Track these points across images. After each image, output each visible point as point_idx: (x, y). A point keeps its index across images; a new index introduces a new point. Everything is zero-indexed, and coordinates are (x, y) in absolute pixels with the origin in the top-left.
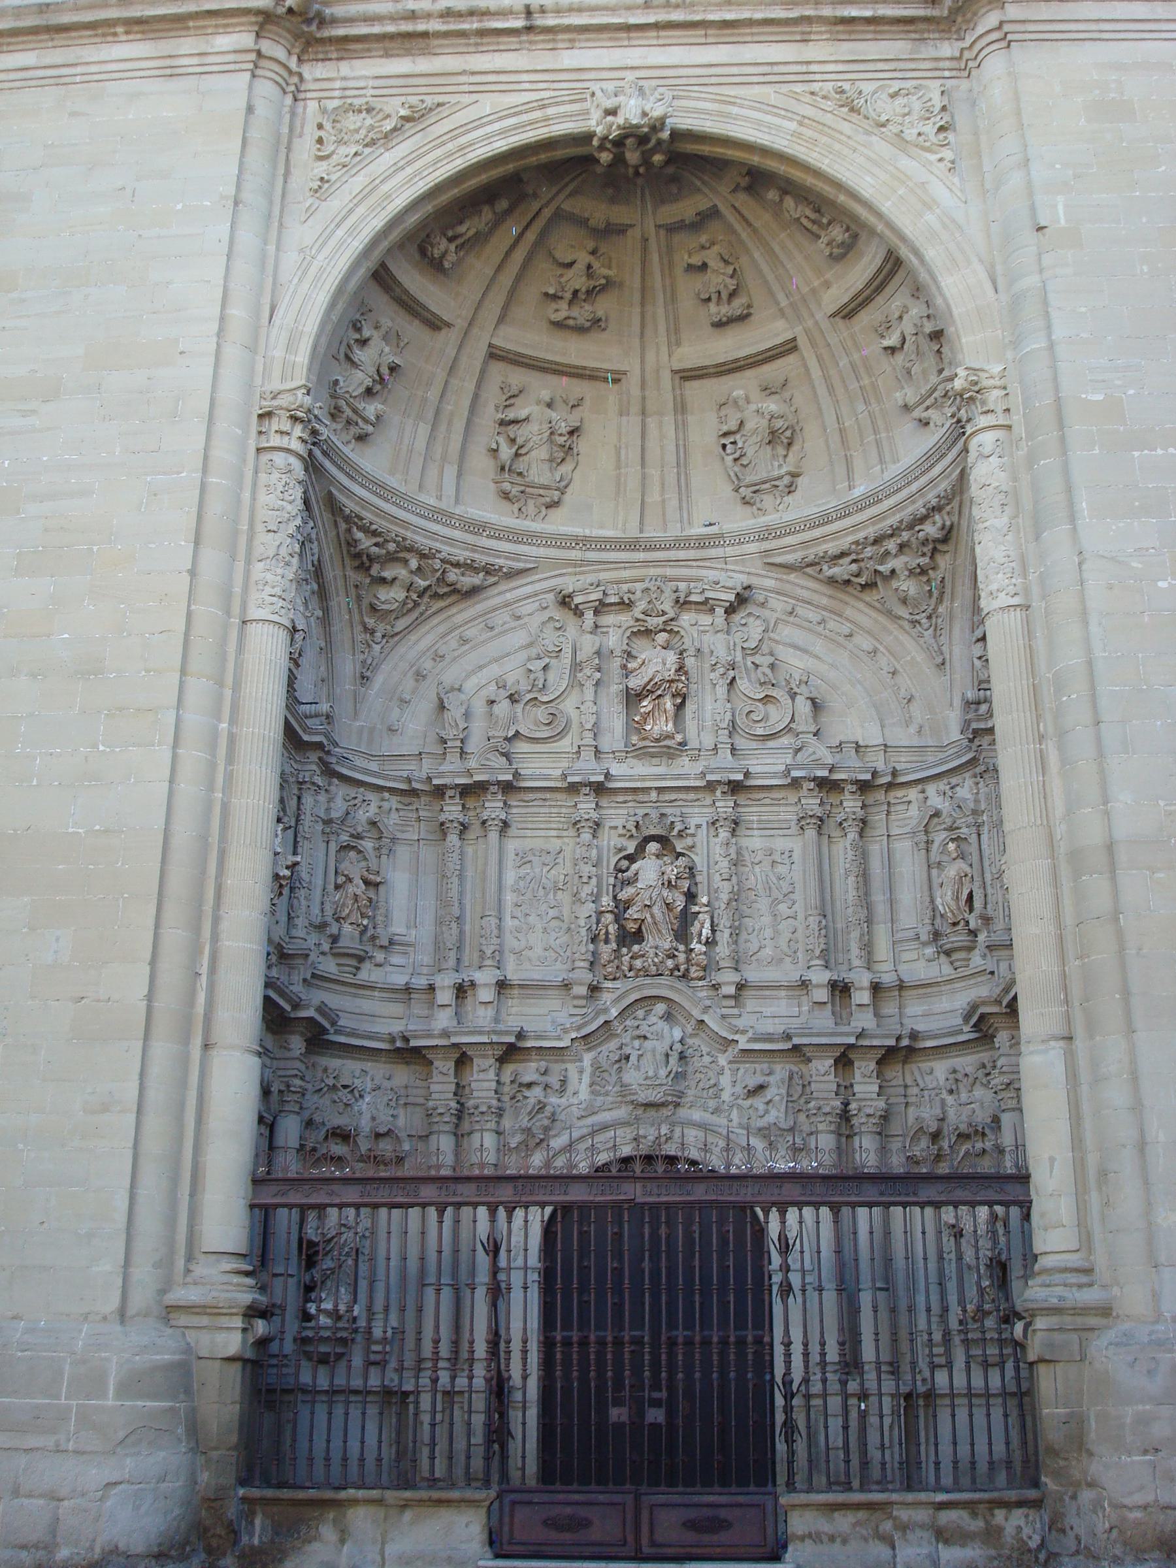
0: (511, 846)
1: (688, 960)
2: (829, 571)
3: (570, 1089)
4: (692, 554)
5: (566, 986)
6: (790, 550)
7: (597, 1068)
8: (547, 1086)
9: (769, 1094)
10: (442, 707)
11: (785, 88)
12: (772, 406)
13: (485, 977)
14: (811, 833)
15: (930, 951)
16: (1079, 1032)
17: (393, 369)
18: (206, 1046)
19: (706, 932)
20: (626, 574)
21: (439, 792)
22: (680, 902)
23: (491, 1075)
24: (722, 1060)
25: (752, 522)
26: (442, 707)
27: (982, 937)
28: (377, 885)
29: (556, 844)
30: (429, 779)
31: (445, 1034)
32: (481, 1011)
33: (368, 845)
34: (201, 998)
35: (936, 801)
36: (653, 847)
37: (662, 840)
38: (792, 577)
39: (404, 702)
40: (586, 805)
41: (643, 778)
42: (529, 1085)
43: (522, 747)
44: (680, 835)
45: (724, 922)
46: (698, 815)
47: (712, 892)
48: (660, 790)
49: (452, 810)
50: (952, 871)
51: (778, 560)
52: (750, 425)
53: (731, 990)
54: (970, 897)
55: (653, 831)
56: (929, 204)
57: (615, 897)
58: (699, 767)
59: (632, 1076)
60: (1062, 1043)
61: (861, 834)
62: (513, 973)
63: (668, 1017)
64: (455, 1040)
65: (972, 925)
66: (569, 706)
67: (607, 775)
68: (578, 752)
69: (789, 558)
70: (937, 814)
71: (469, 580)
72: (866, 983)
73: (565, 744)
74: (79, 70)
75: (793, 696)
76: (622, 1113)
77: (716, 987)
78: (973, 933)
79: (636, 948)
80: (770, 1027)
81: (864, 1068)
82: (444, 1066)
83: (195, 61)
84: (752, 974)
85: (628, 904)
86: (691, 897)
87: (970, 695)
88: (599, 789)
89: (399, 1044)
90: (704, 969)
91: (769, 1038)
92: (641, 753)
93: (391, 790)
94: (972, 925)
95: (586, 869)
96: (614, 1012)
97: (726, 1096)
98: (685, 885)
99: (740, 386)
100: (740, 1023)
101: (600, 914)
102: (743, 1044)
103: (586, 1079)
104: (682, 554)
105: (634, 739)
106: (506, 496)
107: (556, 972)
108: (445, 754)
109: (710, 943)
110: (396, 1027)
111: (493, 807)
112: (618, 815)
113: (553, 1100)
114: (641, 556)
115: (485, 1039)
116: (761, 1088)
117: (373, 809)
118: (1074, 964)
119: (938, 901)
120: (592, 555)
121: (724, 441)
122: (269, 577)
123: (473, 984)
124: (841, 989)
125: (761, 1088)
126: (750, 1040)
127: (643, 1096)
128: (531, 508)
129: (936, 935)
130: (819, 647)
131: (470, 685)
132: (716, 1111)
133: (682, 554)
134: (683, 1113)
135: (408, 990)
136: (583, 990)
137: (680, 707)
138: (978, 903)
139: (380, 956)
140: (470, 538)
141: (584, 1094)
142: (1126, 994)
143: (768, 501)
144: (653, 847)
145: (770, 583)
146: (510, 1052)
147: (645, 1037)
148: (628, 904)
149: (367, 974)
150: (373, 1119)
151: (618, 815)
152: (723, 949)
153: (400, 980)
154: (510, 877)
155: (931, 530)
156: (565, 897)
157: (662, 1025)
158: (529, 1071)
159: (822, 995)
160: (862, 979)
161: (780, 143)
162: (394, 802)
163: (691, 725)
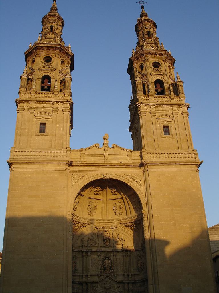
0: (91, 258)
1: (111, 272)
2: (126, 225)
3: (98, 286)
4: (110, 222)
5: (98, 275)
6: (122, 222)
7: (101, 284)
8: (96, 287)
9: (121, 287)
10: (82, 241)
11: (124, 174)
12: (120, 204)
13: (89, 274)
14: (124, 257)
15: (137, 271)
16: (154, 284)
17: (78, 202)
18: (68, 287)
19: (113, 268)
20: (103, 224)
21: (82, 252)
22: (110, 266)
23: (90, 286)
24: (115, 283)
25: (117, 218)
26: (82, 241)
27: (143, 270)
28: (76, 263)
29: (96, 258)
30: (81, 250)
31: (85, 281)
32: (88, 278)
33: (75, 258)
34: (67, 282)
35: (138, 253)
36: (107, 258)
37: (108, 258)
38: (122, 225)
39: (77, 240)
40: (99, 253)
41: (106, 250)
42: (94, 287)
43: (92, 246)
44: (110, 257)
45: (115, 267)
46: (112, 254)
47: (114, 264)
48: (108, 251)
49: (84, 254)
50: (140, 262)
51: (121, 223)
52: (118, 206)
53: (116, 275)
54: (142, 265)
55: (107, 256)
56: (139, 190)
57: (103, 264)
58: (112, 249)
59: (106, 286)
60: (152, 285)
61: (130, 257)
62: (92, 274)
63: (109, 279)
64: (86, 282)
65: (142, 268)
66: (97, 241)
67: (102, 250)
68: (98, 247)
69: (122, 223)
70: (138, 255)
71: (85, 225)
72: (131, 274)
73: (97, 245)
74: (45, 169)
75: (122, 240)
76: (104, 290)
77: (114, 275)
78: (143, 269)
79: (106, 271)
80: (120, 280)
81: (131, 284)
82: (84, 285)
83: (59, 169)
84: (118, 273)
85: (104, 266)
86: (111, 265)
87: (142, 243)
88: (101, 251)
89: (80, 282)
90: (113, 273)
91: (120, 281)
92: (105, 247)
93: (77, 251)
94: (142, 268)
95: (100, 261)
96: (103, 278)
97: (115, 288)
98: (111, 263)
99: (116, 201)
100: (117, 279)
101: (101, 267)
102: (117, 282)
103: (100, 286)
104: (109, 222)
105: (104, 245)
106: (89, 214)
107: (96, 273)
108: (83, 247)
109: (114, 270)
110: (78, 280)
111: (89, 254)
112: (102, 254)
113: (96, 288)
114: (105, 222)
115: (89, 282)
116: (120, 287)
117: (75, 254)
118: (153, 277)
119: (138, 265)
120: (99, 222)
121: (114, 207)
122: (71, 234)
123: (87, 275)
124: (128, 275)
125: (120, 287)
126: (118, 281)
127: (107, 288)
128: (91, 215)
129: (138, 269)
130: (125, 233)
131: (85, 238)
132: (114, 289)
133: (109, 222)
134: (111, 290)
135: (79, 276)
136: (99, 276)
137: (109, 241)
138: (143, 266)
139: (76, 272)
140: (86, 221)
141: (100, 288)
142: (158, 281)
143: (119, 215)
144: (107, 258)
145: (119, 225)
146: (92, 283)
147: (107, 281)
148: (104, 266)
149: (76, 274)
150: (77, 291)
151: (102, 254)
152: (115, 271)
153: (79, 274)
154: (91, 262)
155: (138, 222)
156: (97, 264)
157: (109, 280)
158: (94, 285)
159: (126, 276)
160: (130, 274)
161: (123, 181)
162: (77, 253)
163: (111, 244)
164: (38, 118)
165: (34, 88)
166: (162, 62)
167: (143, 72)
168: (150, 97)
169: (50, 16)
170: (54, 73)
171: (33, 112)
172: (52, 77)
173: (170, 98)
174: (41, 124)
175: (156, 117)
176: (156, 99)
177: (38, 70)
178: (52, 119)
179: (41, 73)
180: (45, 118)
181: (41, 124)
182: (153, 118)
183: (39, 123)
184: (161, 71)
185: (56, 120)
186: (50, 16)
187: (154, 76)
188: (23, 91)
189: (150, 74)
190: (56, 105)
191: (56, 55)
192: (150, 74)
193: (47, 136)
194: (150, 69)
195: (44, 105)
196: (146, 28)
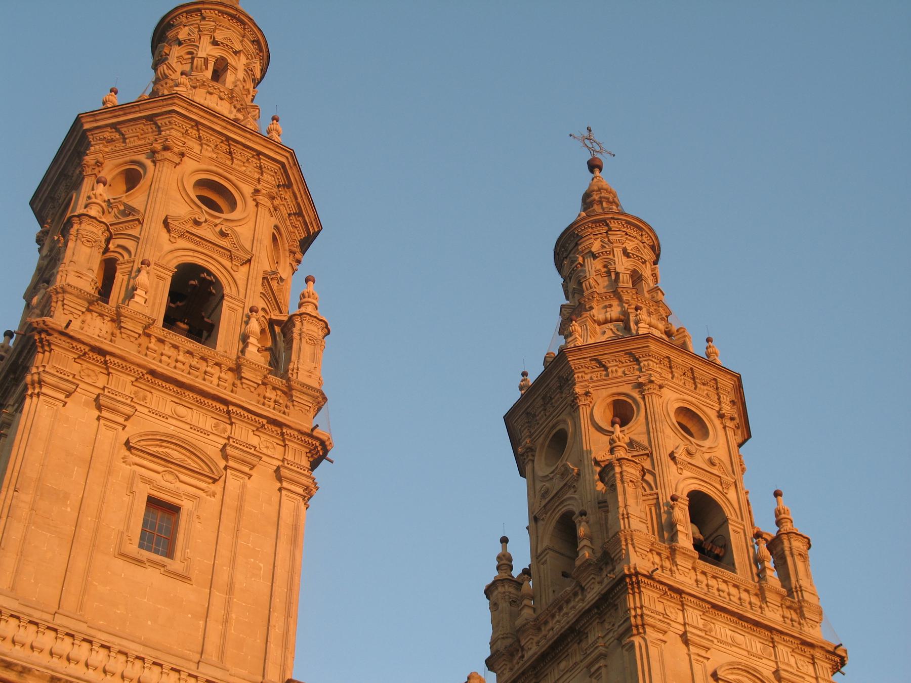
164: (145, 463)
165: (142, 301)
166: (717, 422)
167: (636, 430)
168: (679, 560)
169: (223, 13)
170: (241, 274)
171: (121, 420)
172: (227, 291)
173: (763, 599)
174: (153, 503)
175: (710, 667)
176: (701, 577)
177: (166, 223)
178: (219, 496)
179: (176, 246)
180: (183, 478)
181: (153, 503)
182: (697, 668)
183: (143, 492)
184: (717, 462)
185: (240, 509)
186: (223, 13)
187: (686, 473)
188: (80, 294)
189: (672, 456)
190: (243, 433)
191: (257, 191)
192: (672, 456)
193: (184, 578)
194: (668, 431)
195: (181, 410)
196: (626, 253)
